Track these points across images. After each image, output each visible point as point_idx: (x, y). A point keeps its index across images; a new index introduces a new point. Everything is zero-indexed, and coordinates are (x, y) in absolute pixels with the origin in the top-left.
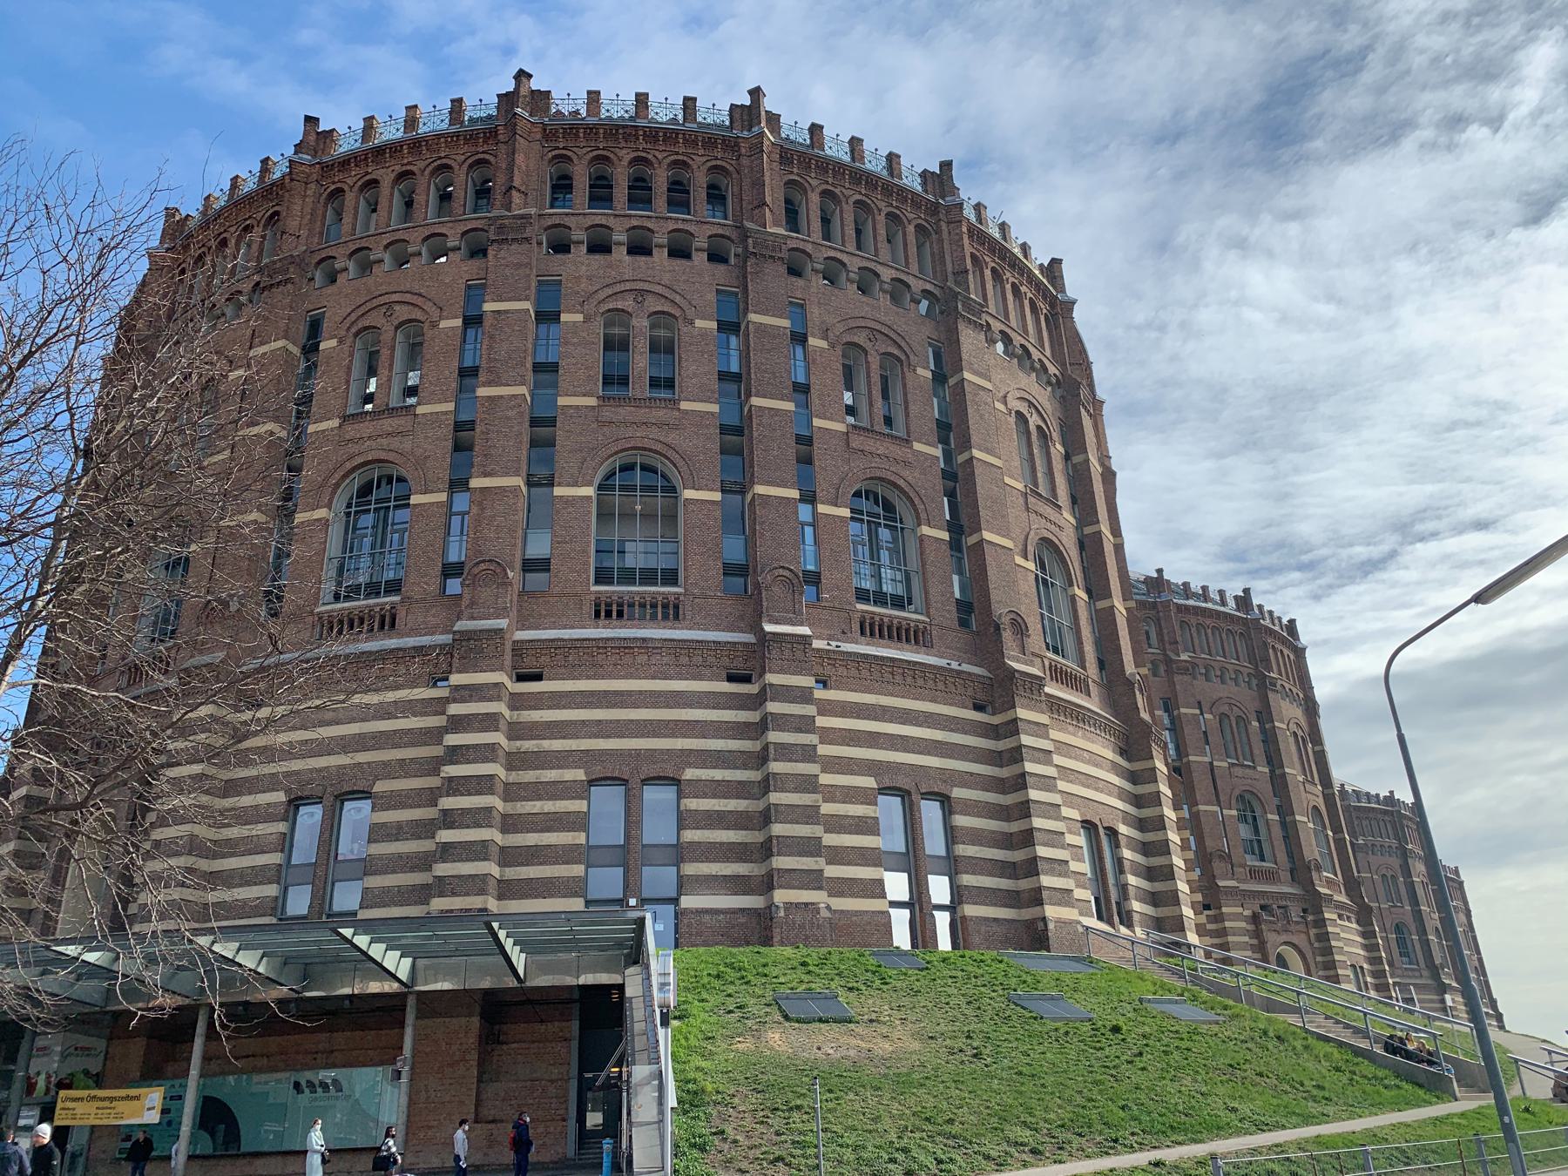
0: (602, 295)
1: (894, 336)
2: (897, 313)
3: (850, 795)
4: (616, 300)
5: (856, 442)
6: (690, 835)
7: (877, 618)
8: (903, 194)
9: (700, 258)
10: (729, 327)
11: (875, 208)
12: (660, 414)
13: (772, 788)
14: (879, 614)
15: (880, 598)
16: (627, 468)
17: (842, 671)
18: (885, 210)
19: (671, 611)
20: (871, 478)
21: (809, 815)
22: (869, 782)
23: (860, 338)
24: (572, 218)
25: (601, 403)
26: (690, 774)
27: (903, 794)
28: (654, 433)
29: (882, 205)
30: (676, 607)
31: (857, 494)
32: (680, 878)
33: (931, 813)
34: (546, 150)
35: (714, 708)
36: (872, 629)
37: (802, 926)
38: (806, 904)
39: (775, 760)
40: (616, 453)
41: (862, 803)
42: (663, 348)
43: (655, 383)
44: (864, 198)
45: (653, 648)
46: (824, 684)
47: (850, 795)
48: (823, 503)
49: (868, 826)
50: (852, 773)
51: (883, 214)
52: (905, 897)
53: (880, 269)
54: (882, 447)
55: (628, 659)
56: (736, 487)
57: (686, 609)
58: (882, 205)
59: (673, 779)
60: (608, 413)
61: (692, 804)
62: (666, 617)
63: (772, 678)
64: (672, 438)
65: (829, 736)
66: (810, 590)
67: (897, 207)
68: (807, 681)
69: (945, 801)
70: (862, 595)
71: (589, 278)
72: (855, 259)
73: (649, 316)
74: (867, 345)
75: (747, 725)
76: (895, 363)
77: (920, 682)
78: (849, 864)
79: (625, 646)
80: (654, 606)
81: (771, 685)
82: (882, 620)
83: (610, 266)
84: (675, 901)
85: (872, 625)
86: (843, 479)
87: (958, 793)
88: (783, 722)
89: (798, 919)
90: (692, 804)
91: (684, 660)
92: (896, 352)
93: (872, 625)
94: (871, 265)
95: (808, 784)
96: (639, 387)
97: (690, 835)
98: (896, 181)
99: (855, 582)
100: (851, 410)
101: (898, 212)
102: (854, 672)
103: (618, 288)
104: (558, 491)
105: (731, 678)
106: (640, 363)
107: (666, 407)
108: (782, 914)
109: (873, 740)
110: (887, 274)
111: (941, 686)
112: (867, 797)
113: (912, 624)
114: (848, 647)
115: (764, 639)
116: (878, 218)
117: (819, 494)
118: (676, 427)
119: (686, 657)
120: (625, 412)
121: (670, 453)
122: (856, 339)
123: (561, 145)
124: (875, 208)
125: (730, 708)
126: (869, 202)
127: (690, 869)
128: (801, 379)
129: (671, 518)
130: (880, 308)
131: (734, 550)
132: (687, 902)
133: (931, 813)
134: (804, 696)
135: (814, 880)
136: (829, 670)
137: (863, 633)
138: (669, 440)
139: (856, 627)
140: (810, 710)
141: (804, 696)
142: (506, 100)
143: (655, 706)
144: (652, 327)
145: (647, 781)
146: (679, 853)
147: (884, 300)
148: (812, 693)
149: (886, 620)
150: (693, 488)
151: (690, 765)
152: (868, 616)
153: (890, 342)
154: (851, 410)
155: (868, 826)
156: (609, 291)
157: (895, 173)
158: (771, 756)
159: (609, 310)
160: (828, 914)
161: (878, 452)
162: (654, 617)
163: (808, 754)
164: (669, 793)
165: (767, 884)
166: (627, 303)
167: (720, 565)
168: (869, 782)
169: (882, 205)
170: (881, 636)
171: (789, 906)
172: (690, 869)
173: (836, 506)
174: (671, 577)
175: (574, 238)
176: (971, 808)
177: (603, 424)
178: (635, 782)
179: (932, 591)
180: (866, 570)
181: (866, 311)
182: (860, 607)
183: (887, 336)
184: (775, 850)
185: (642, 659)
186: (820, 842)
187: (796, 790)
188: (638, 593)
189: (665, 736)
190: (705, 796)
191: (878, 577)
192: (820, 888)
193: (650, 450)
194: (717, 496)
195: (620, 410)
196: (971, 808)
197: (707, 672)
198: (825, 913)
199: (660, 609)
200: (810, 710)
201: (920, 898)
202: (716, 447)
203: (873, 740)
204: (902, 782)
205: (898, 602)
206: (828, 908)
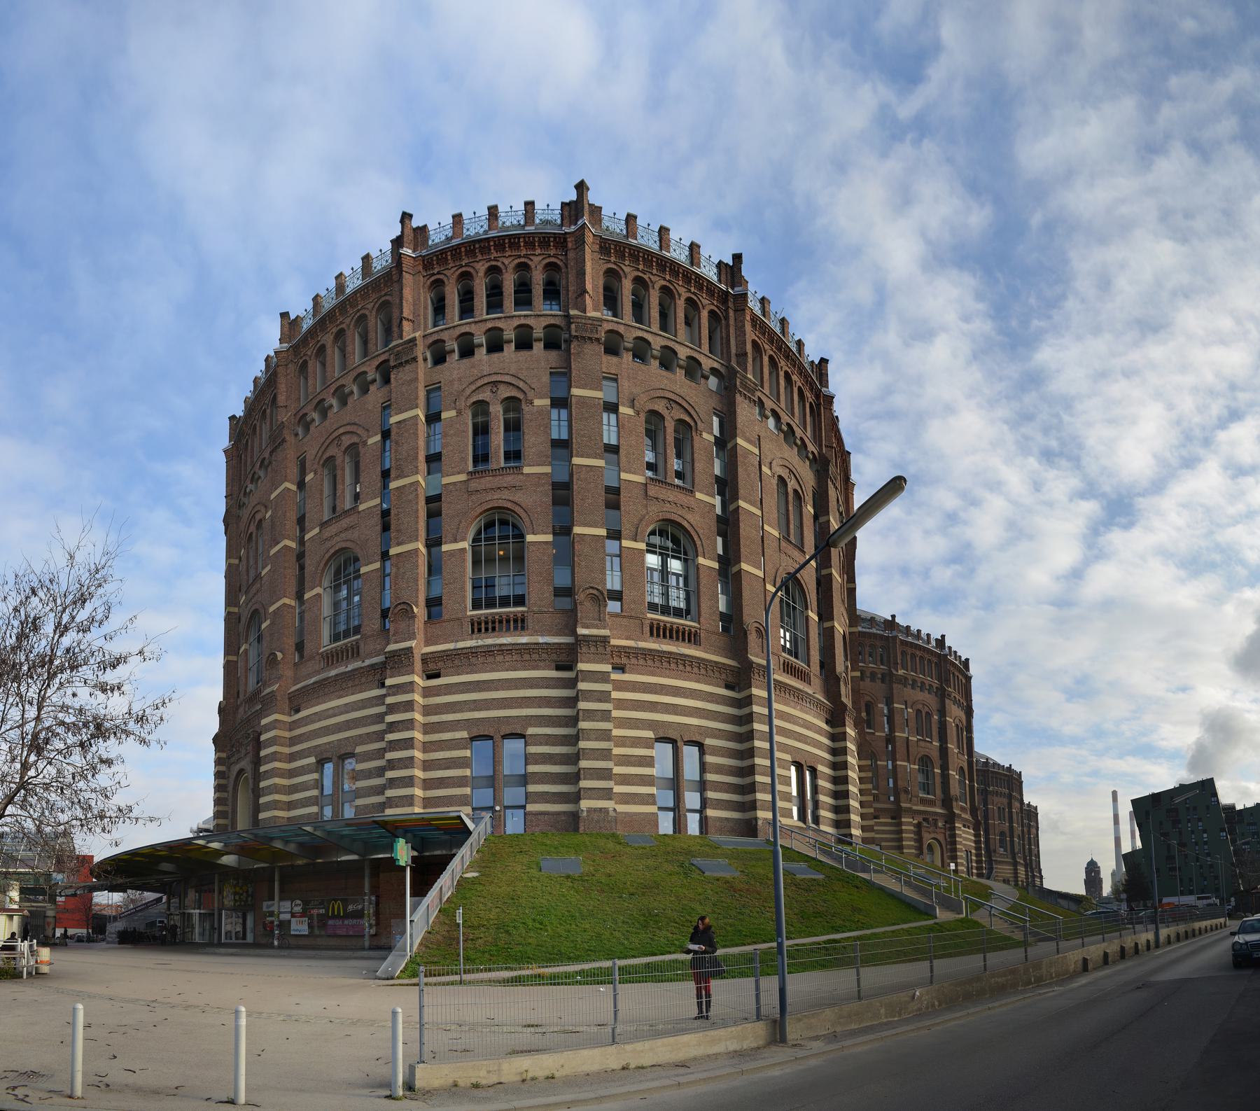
0: (468, 391)
1: (686, 406)
2: (690, 387)
3: (636, 742)
4: (479, 394)
5: (653, 490)
6: (532, 768)
7: (662, 624)
8: (700, 281)
9: (538, 347)
10: (560, 403)
11: (676, 293)
12: (509, 479)
13: (581, 738)
14: (663, 621)
15: (666, 610)
16: (489, 525)
17: (634, 661)
18: (685, 295)
19: (519, 624)
20: (663, 520)
21: (605, 754)
22: (650, 734)
23: (660, 407)
24: (446, 332)
25: (470, 477)
26: (531, 731)
27: (673, 741)
28: (506, 495)
29: (683, 292)
30: (523, 621)
31: (653, 533)
32: (526, 793)
33: (690, 754)
34: (426, 279)
35: (546, 688)
36: (658, 631)
37: (598, 821)
38: (601, 809)
39: (583, 721)
40: (481, 514)
41: (644, 748)
42: (513, 427)
43: (508, 456)
44: (668, 284)
45: (507, 650)
46: (621, 668)
47: (636, 742)
48: (626, 539)
49: (648, 761)
50: (638, 728)
51: (683, 299)
52: (671, 805)
53: (677, 348)
54: (671, 495)
55: (490, 659)
56: (563, 531)
57: (530, 622)
58: (682, 290)
59: (521, 734)
60: (474, 485)
61: (533, 749)
62: (516, 628)
63: (582, 666)
64: (518, 497)
65: (621, 704)
66: (613, 606)
67: (694, 293)
68: (608, 668)
69: (700, 746)
70: (653, 607)
71: (460, 379)
72: (658, 338)
73: (501, 403)
74: (665, 412)
75: (568, 698)
76: (685, 429)
77: (688, 668)
78: (633, 785)
79: (488, 652)
80: (508, 621)
81: (581, 671)
82: (665, 625)
83: (473, 367)
84: (524, 807)
85: (658, 629)
86: (641, 520)
87: (708, 742)
88: (590, 696)
89: (596, 818)
90: (533, 749)
91: (527, 657)
92: (687, 419)
93: (658, 629)
94: (671, 344)
95: (605, 735)
96: (498, 460)
97: (532, 768)
98: (695, 269)
99: (648, 599)
100: (650, 466)
101: (695, 298)
102: (642, 662)
103: (479, 383)
104: (445, 548)
105: (558, 668)
106: (498, 439)
107: (514, 473)
108: (585, 814)
109: (653, 707)
110: (683, 353)
111: (703, 671)
112: (647, 744)
113: (687, 629)
114: (642, 644)
115: (581, 641)
116: (678, 301)
117: (624, 533)
118: (520, 488)
119: (526, 654)
120: (487, 482)
121: (517, 509)
122: (656, 408)
123: (435, 271)
124: (676, 293)
125: (557, 688)
126: (672, 287)
127: (532, 788)
128: (614, 442)
129: (520, 558)
130: (677, 382)
131: (562, 579)
132: (530, 808)
133: (690, 754)
134: (603, 678)
135: (607, 794)
136: (624, 660)
137: (652, 634)
138: (516, 499)
139: (647, 629)
140: (608, 687)
141: (603, 678)
142: (397, 243)
143: (509, 688)
144: (506, 411)
145: (505, 737)
146: (524, 780)
147: (680, 373)
148: (609, 676)
149: (668, 625)
150: (533, 533)
151: (531, 725)
152: (655, 623)
153: (682, 411)
154: (650, 466)
155: (648, 761)
156: (474, 387)
157: (695, 261)
158: (581, 718)
159: (474, 403)
160: (614, 815)
161: (669, 499)
162: (508, 629)
163: (606, 715)
164: (518, 744)
165: (576, 797)
166: (485, 395)
167: (552, 589)
168: (650, 734)
169: (682, 290)
170: (665, 637)
171: (590, 810)
172: (532, 788)
173: (636, 541)
174: (520, 600)
175: (447, 348)
176: (717, 751)
177: (470, 493)
178: (497, 737)
179: (703, 605)
180: (657, 589)
181: (665, 383)
182: (649, 616)
183: (680, 405)
184: (582, 776)
185: (499, 658)
186: (611, 771)
187: (596, 739)
188: (497, 614)
189: (516, 708)
190: (541, 744)
191: (666, 595)
192: (610, 799)
193: (504, 508)
194: (549, 538)
195: (483, 480)
196: (717, 751)
197: (541, 664)
198: (612, 813)
199: (512, 623)
200: (608, 687)
201: (678, 806)
202: (549, 500)
203: (653, 707)
204: (672, 734)
205: (678, 613)
206: (615, 810)
